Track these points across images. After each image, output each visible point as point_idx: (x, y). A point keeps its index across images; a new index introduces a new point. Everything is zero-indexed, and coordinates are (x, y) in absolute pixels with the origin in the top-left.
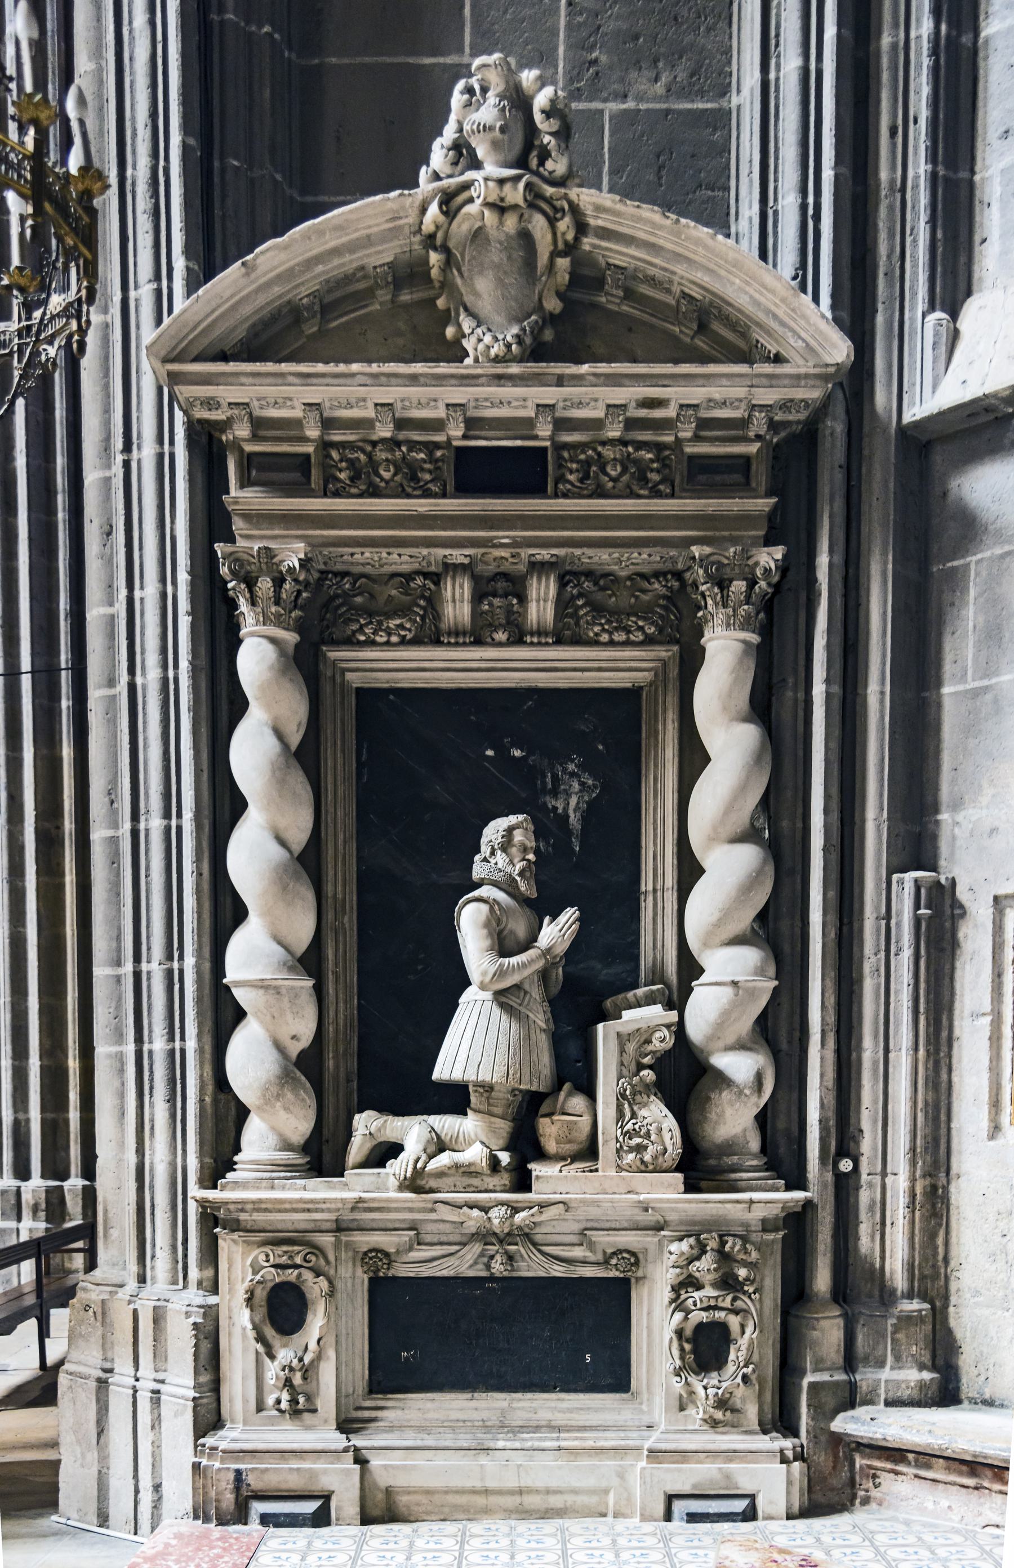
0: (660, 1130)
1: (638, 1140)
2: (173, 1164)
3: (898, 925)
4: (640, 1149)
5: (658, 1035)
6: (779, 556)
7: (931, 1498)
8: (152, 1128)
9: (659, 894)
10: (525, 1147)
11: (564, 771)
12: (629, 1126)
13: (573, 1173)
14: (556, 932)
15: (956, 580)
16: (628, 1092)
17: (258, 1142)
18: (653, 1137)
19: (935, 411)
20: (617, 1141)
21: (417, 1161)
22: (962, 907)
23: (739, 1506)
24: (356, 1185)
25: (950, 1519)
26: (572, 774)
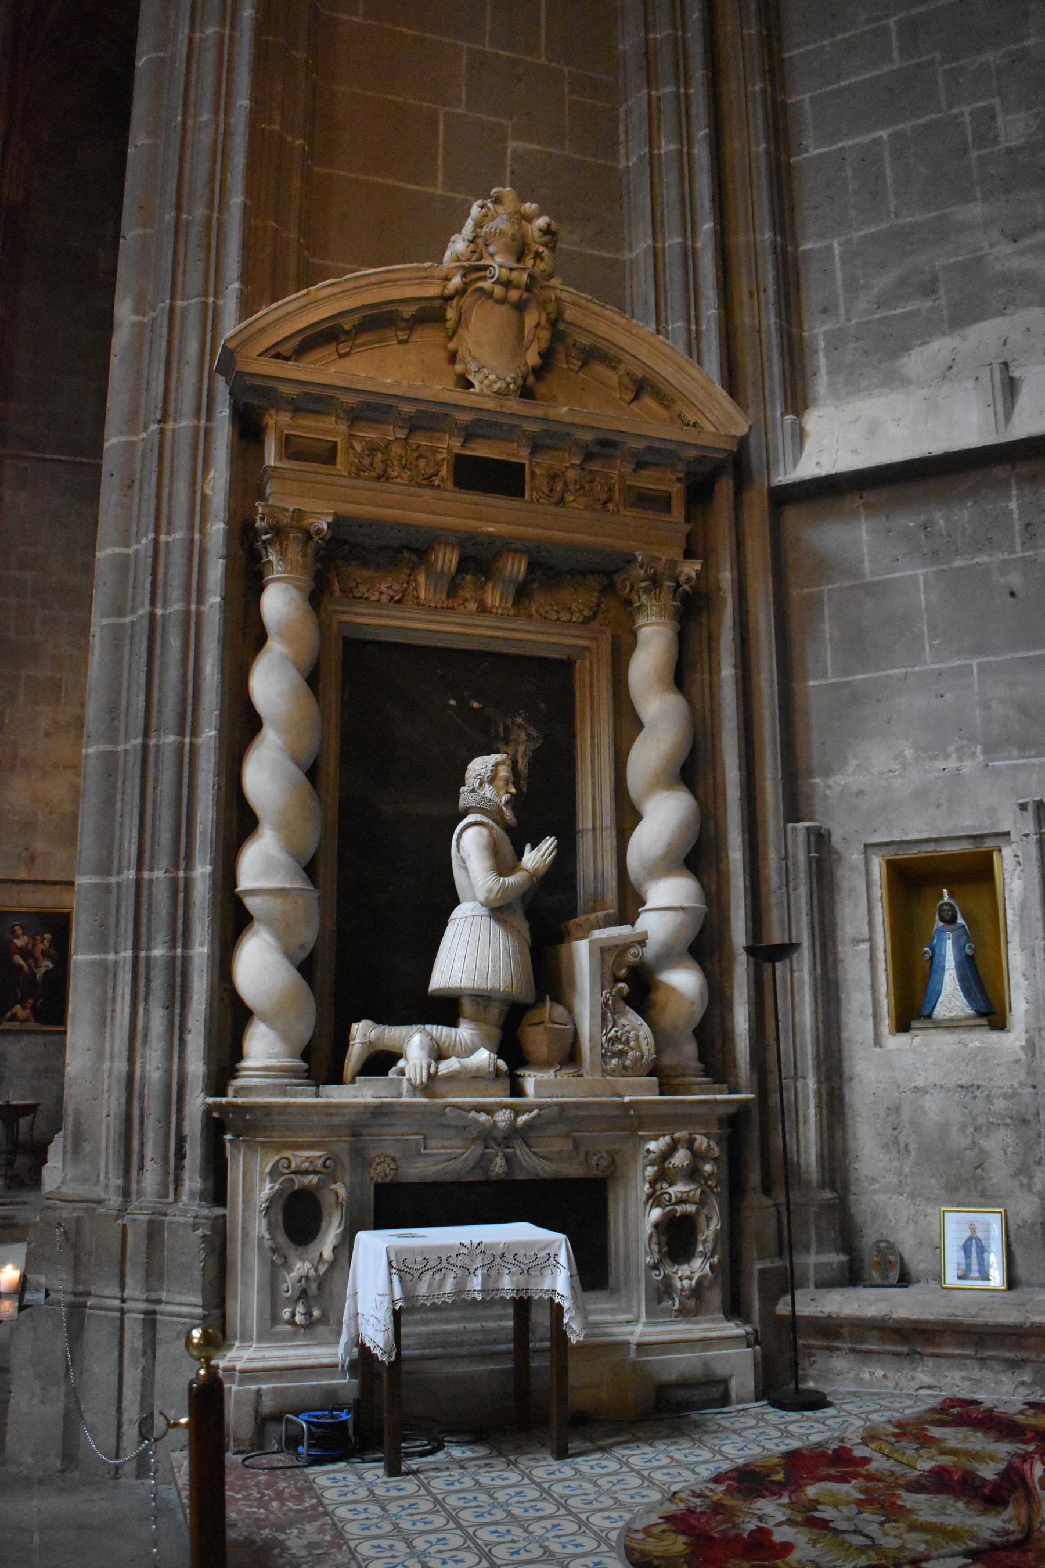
0: (637, 1037)
1: (620, 1047)
2: (168, 1072)
3: (795, 864)
4: (621, 1054)
5: (632, 951)
7: (866, 1369)
8: (146, 1035)
10: (513, 1053)
12: (612, 1033)
13: (565, 1078)
15: (814, 602)
16: (610, 1002)
17: (263, 1049)
18: (632, 1044)
20: (603, 1047)
21: (429, 1067)
22: (837, 852)
23: (716, 1392)
25: (886, 1387)
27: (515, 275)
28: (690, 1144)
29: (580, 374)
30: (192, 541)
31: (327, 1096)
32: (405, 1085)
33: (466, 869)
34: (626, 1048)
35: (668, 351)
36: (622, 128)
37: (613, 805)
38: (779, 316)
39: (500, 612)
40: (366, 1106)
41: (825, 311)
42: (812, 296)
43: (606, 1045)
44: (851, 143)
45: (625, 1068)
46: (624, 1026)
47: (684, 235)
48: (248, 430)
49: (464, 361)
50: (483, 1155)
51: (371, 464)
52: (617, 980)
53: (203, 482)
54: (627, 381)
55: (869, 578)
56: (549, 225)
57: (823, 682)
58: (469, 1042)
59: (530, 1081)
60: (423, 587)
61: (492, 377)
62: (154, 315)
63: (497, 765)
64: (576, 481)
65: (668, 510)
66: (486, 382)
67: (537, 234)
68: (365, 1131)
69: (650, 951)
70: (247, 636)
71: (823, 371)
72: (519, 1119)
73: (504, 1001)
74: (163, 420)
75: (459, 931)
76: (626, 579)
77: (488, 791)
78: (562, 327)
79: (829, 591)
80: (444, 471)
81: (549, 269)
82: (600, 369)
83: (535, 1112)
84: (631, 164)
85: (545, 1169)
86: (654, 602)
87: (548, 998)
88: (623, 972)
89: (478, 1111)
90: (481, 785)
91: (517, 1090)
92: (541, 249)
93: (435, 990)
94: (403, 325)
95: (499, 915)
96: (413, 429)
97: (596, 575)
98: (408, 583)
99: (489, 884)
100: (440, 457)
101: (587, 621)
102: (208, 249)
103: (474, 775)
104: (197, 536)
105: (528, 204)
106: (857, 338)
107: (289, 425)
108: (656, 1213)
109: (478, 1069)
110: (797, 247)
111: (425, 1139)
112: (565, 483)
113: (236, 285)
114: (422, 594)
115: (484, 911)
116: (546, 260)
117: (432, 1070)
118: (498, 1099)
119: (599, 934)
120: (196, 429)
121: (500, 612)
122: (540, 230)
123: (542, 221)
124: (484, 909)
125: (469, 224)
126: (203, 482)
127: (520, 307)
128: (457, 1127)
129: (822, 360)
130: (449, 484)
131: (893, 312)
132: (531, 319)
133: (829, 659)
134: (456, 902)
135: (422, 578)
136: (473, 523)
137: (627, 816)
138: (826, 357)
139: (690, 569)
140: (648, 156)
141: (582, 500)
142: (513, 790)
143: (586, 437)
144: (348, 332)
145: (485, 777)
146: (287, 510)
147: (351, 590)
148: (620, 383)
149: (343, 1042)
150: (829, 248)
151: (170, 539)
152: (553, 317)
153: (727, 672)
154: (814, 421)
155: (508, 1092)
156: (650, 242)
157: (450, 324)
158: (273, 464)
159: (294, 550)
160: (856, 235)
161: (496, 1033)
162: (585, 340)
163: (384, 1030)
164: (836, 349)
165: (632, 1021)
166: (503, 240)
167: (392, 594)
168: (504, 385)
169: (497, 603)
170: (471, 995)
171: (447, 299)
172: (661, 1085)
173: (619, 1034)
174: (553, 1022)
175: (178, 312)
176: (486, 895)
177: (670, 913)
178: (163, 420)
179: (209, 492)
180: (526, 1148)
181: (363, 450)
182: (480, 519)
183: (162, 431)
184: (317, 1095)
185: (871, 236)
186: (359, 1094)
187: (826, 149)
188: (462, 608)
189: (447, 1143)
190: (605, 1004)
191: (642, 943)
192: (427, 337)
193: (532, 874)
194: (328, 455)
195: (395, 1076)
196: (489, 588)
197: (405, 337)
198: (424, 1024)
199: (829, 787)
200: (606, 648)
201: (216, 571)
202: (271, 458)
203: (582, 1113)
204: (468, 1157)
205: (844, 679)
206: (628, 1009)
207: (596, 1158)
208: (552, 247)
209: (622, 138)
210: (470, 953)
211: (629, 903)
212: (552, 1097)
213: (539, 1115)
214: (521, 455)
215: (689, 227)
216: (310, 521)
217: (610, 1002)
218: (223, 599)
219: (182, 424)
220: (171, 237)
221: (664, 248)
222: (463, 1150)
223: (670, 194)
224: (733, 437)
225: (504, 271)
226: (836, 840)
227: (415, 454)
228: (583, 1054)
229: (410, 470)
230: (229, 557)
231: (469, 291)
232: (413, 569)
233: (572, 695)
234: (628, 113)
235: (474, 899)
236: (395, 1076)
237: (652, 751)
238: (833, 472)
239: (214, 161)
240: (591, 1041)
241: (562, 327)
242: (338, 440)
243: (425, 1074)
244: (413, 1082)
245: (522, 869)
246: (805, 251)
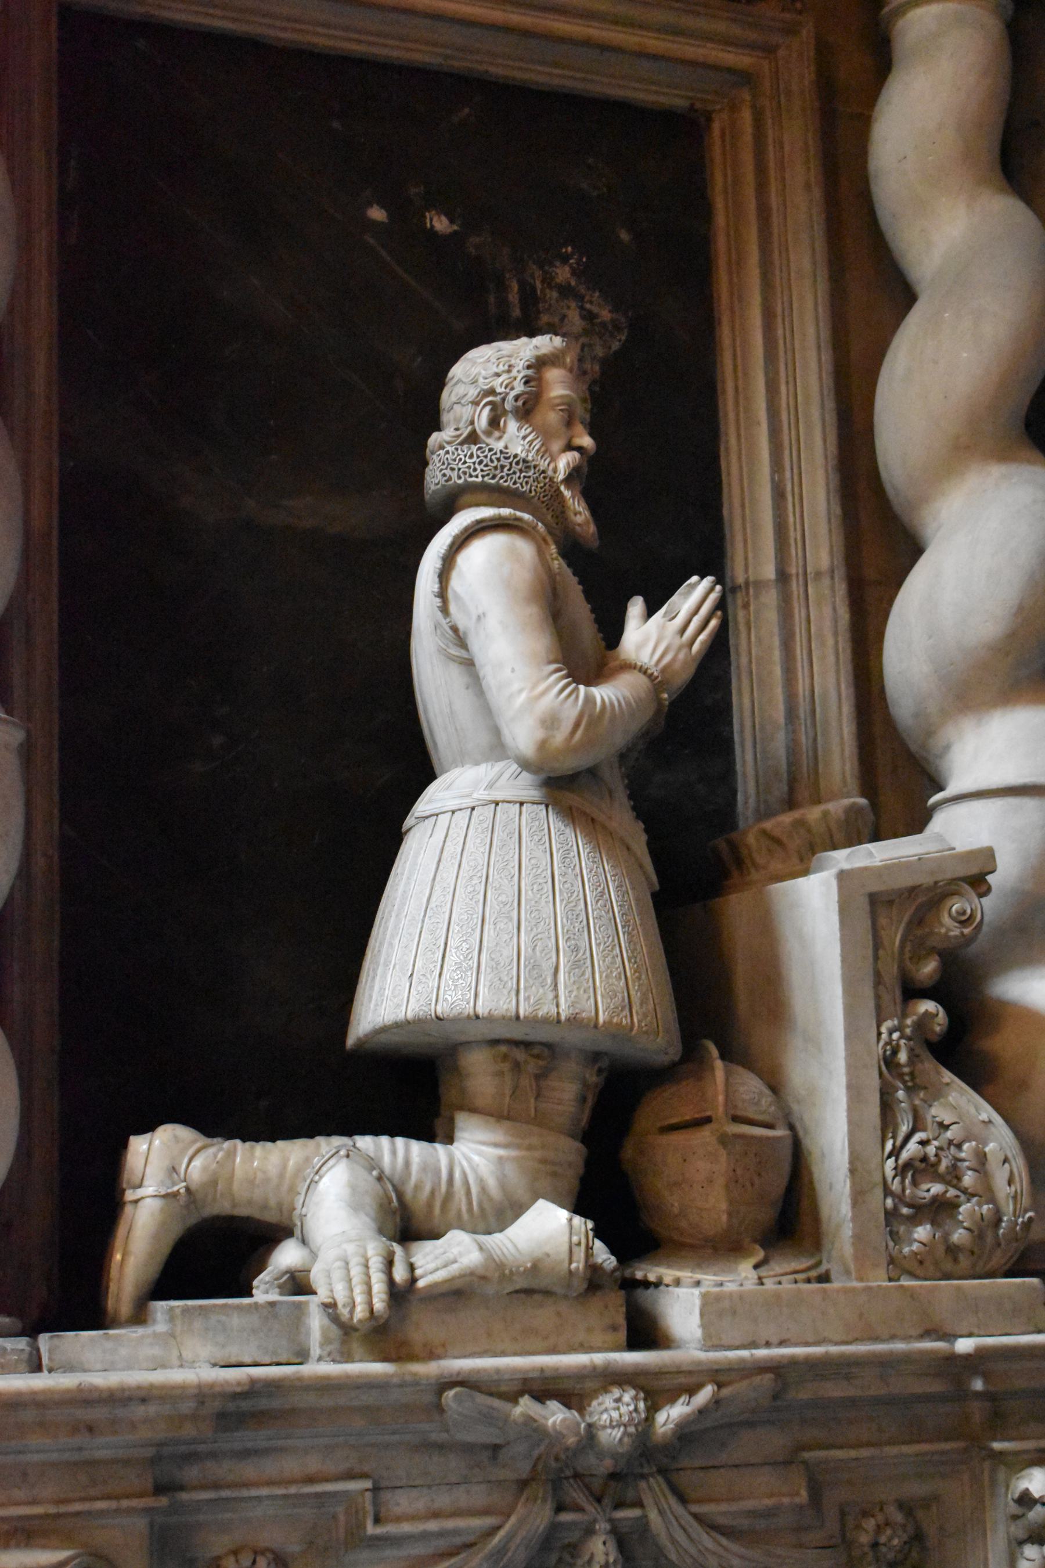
0: (982, 1158)
1: (936, 1188)
4: (940, 1210)
9: (795, 587)
11: (548, 281)
12: (912, 1148)
13: (787, 1286)
14: (655, 637)
16: (903, 1057)
18: (968, 1179)
20: (887, 1192)
21: (389, 1263)
26: (566, 291)
31: (69, 1368)
32: (316, 1323)
33: (469, 664)
34: (952, 1192)
37: (837, 510)
40: (203, 1394)
43: (896, 1186)
45: (953, 1251)
46: (944, 1127)
50: (555, 1527)
52: (911, 992)
58: (492, 1183)
59: (684, 1302)
63: (540, 364)
68: (192, 1473)
72: (661, 1417)
73: (595, 1057)
75: (453, 848)
77: (516, 439)
83: (705, 1394)
87: (714, 1052)
88: (929, 969)
89: (541, 1396)
90: (494, 423)
91: (644, 1332)
93: (384, 1029)
95: (573, 799)
99: (549, 701)
103: (473, 393)
109: (535, 1268)
111: (376, 1489)
115: (525, 786)
117: (400, 1274)
118: (599, 1358)
119: (843, 858)
124: (526, 777)
128: (468, 1448)
134: (421, 771)
137: (880, 545)
142: (586, 441)
145: (499, 397)
149: (99, 1199)
155: (622, 1336)
161: (570, 1152)
163: (231, 1154)
170: (495, 1042)
173: (931, 1150)
174: (736, 1119)
176: (540, 734)
180: (673, 1501)
184: (36, 1366)
186: (167, 1355)
189: (443, 1500)
190: (889, 1061)
191: (978, 883)
193: (657, 683)
195: (274, 1296)
198: (349, 1131)
200: (799, 74)
203: (835, 1390)
204: (511, 1537)
206: (947, 1076)
207: (870, 1524)
210: (481, 913)
212: (753, 1345)
213: (717, 1402)
217: (903, 1057)
222: (489, 1521)
228: (825, 1211)
235: (497, 748)
236: (274, 1296)
240: (852, 1171)
243: (379, 1287)
244: (344, 1312)
245: (628, 666)
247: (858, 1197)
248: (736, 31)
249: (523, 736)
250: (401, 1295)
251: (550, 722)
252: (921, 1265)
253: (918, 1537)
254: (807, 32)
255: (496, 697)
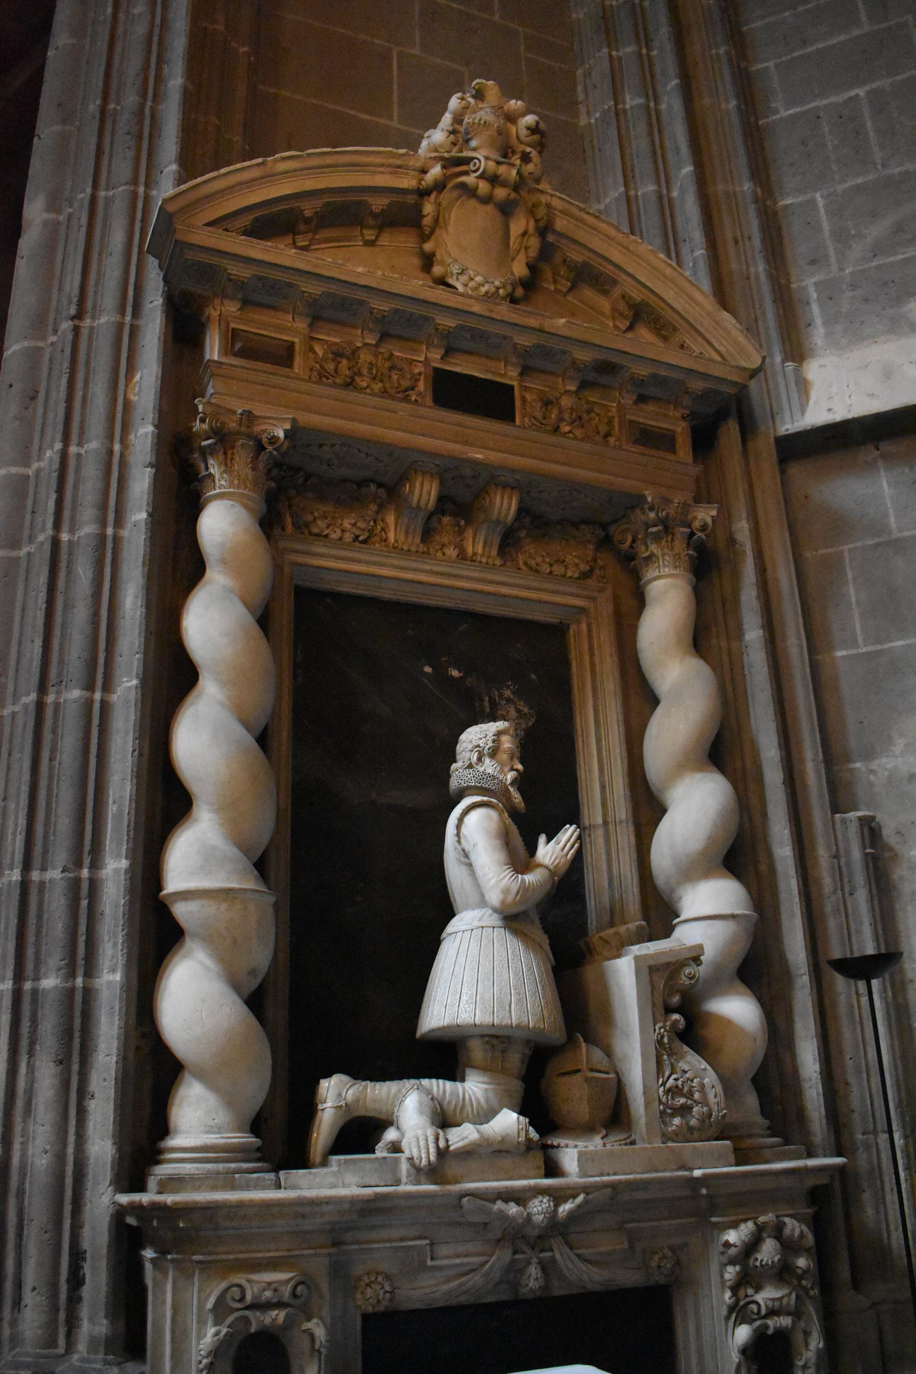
0: (702, 1086)
1: (683, 1100)
2: (60, 1157)
3: (848, 864)
4: (684, 1110)
6: (714, 513)
11: (501, 696)
12: (671, 1082)
13: (616, 1147)
14: (551, 852)
16: (666, 1040)
17: (198, 1119)
18: (697, 1096)
19: (809, 428)
20: (660, 1102)
21: (437, 1139)
22: (891, 849)
24: (335, 1182)
26: (509, 700)
27: (502, 169)
28: (778, 1232)
29: (569, 298)
30: (111, 452)
31: (294, 1187)
32: (404, 1166)
33: (470, 865)
34: (690, 1102)
35: (668, 271)
36: (580, 88)
37: (628, 793)
38: (768, 262)
39: (484, 560)
40: (353, 1201)
41: (813, 262)
42: (798, 250)
43: (664, 1100)
44: (824, 102)
45: (691, 1129)
46: (685, 1072)
47: (658, 183)
48: (184, 330)
49: (442, 263)
50: (513, 1261)
51: (336, 371)
52: (668, 1010)
53: (127, 386)
54: (622, 306)
55: (896, 535)
56: (537, 123)
57: (854, 652)
58: (482, 1100)
59: (570, 1156)
60: (392, 528)
61: (479, 279)
62: (70, 210)
63: (499, 734)
64: (572, 409)
65: (672, 449)
66: (471, 284)
67: (523, 132)
68: (348, 1236)
69: (702, 971)
70: (179, 566)
71: (818, 321)
72: (561, 1209)
73: (528, 1042)
74: (79, 316)
75: (464, 948)
76: (627, 530)
77: (489, 766)
78: (551, 238)
79: (850, 551)
80: (421, 386)
81: (538, 173)
82: (589, 293)
83: (581, 1198)
84: (593, 121)
85: (594, 1277)
86: (666, 550)
87: (582, 1040)
88: (676, 999)
89: (506, 1200)
90: (480, 759)
91: (552, 1169)
92: (528, 150)
93: (433, 1030)
94: (371, 222)
95: (515, 925)
96: (384, 336)
97: (591, 527)
98: (375, 522)
99: (505, 882)
100: (417, 371)
101: (585, 575)
102: (140, 137)
103: (470, 746)
104: (117, 447)
105: (513, 102)
106: (854, 287)
107: (236, 318)
108: (743, 1333)
109: (503, 1140)
110: (775, 203)
111: (432, 1244)
112: (561, 411)
113: (174, 167)
114: (392, 536)
115: (495, 920)
116: (534, 160)
117: (442, 1144)
118: (532, 1182)
119: (636, 950)
120: (120, 326)
121: (484, 560)
122: (528, 128)
123: (530, 119)
124: (496, 916)
125: (447, 118)
126: (127, 386)
127: (506, 210)
128: (472, 1225)
129: (815, 310)
130: (429, 400)
131: (891, 259)
132: (518, 225)
133: (858, 626)
134: (448, 912)
135: (391, 519)
136: (455, 448)
137: (648, 808)
138: (821, 306)
139: (705, 515)
140: (613, 109)
141: (579, 432)
142: (520, 767)
143: (584, 356)
144: (307, 221)
145: (482, 748)
146: (234, 412)
147: (307, 525)
148: (614, 309)
149: (305, 1107)
150: (813, 202)
151: (83, 451)
152: (542, 224)
153: (753, 634)
154: (813, 370)
155: (543, 1172)
156: (622, 189)
157: (427, 221)
158: (216, 358)
159: (242, 458)
160: (840, 188)
161: (517, 1086)
162: (577, 256)
163: (366, 1088)
164: (831, 299)
165: (692, 1062)
166: (489, 133)
167: (358, 532)
168: (493, 289)
169: (480, 551)
170: (482, 1036)
171: (423, 193)
172: (736, 1150)
173: (680, 1083)
174: (592, 1070)
175: (101, 204)
176: (501, 897)
177: (718, 924)
178: (79, 316)
179: (133, 398)
181: (325, 353)
182: (466, 443)
183: (76, 330)
184: (278, 1186)
185: (857, 188)
187: (798, 110)
188: (439, 554)
189: (461, 1249)
190: (660, 1042)
191: (697, 960)
192: (400, 242)
193: (552, 873)
194: (283, 356)
195: (385, 1154)
196: (469, 533)
197: (374, 238)
198: (418, 1077)
199: (873, 772)
200: (606, 609)
201: (141, 483)
202: (213, 349)
203: (640, 1195)
204: (493, 1265)
205: (879, 647)
206: (686, 1048)
207: (657, 1257)
208: (541, 147)
209: (581, 97)
210: (476, 977)
211: (660, 914)
212: (602, 1175)
213: (586, 1202)
214: (510, 375)
215: (663, 175)
216: (263, 427)
217: (666, 1040)
218: (150, 515)
219: (103, 320)
220: (96, 124)
221: (636, 196)
222: (484, 1258)
223: (640, 143)
224: (745, 369)
225: (491, 164)
226: (888, 833)
227: (387, 365)
228: (633, 1112)
229: (382, 381)
230: (157, 466)
231: (449, 186)
232: (381, 507)
233: (567, 664)
234: (588, 74)
235: (483, 902)
236: (385, 1154)
237: (677, 724)
238: (850, 416)
239: (149, 52)
240: (645, 1093)
241: (551, 238)
242: (296, 340)
243: (432, 1150)
244: (417, 1162)
245: (540, 865)
246: (786, 207)
247: (647, 1104)
248: (580, 592)
249: (494, 897)
250: (443, 1153)
251: (506, 891)
252: (676, 1136)
253: (678, 1263)
254: (609, 592)
255: (482, 881)
